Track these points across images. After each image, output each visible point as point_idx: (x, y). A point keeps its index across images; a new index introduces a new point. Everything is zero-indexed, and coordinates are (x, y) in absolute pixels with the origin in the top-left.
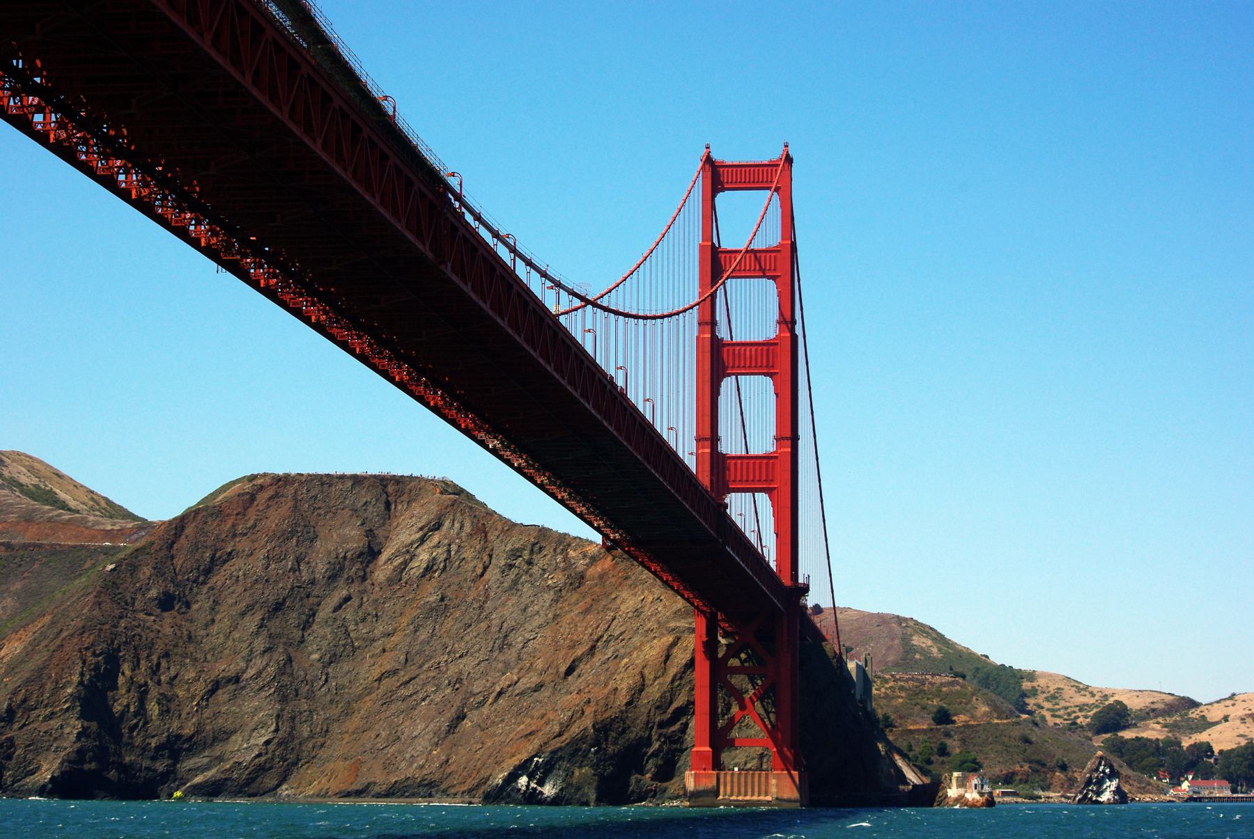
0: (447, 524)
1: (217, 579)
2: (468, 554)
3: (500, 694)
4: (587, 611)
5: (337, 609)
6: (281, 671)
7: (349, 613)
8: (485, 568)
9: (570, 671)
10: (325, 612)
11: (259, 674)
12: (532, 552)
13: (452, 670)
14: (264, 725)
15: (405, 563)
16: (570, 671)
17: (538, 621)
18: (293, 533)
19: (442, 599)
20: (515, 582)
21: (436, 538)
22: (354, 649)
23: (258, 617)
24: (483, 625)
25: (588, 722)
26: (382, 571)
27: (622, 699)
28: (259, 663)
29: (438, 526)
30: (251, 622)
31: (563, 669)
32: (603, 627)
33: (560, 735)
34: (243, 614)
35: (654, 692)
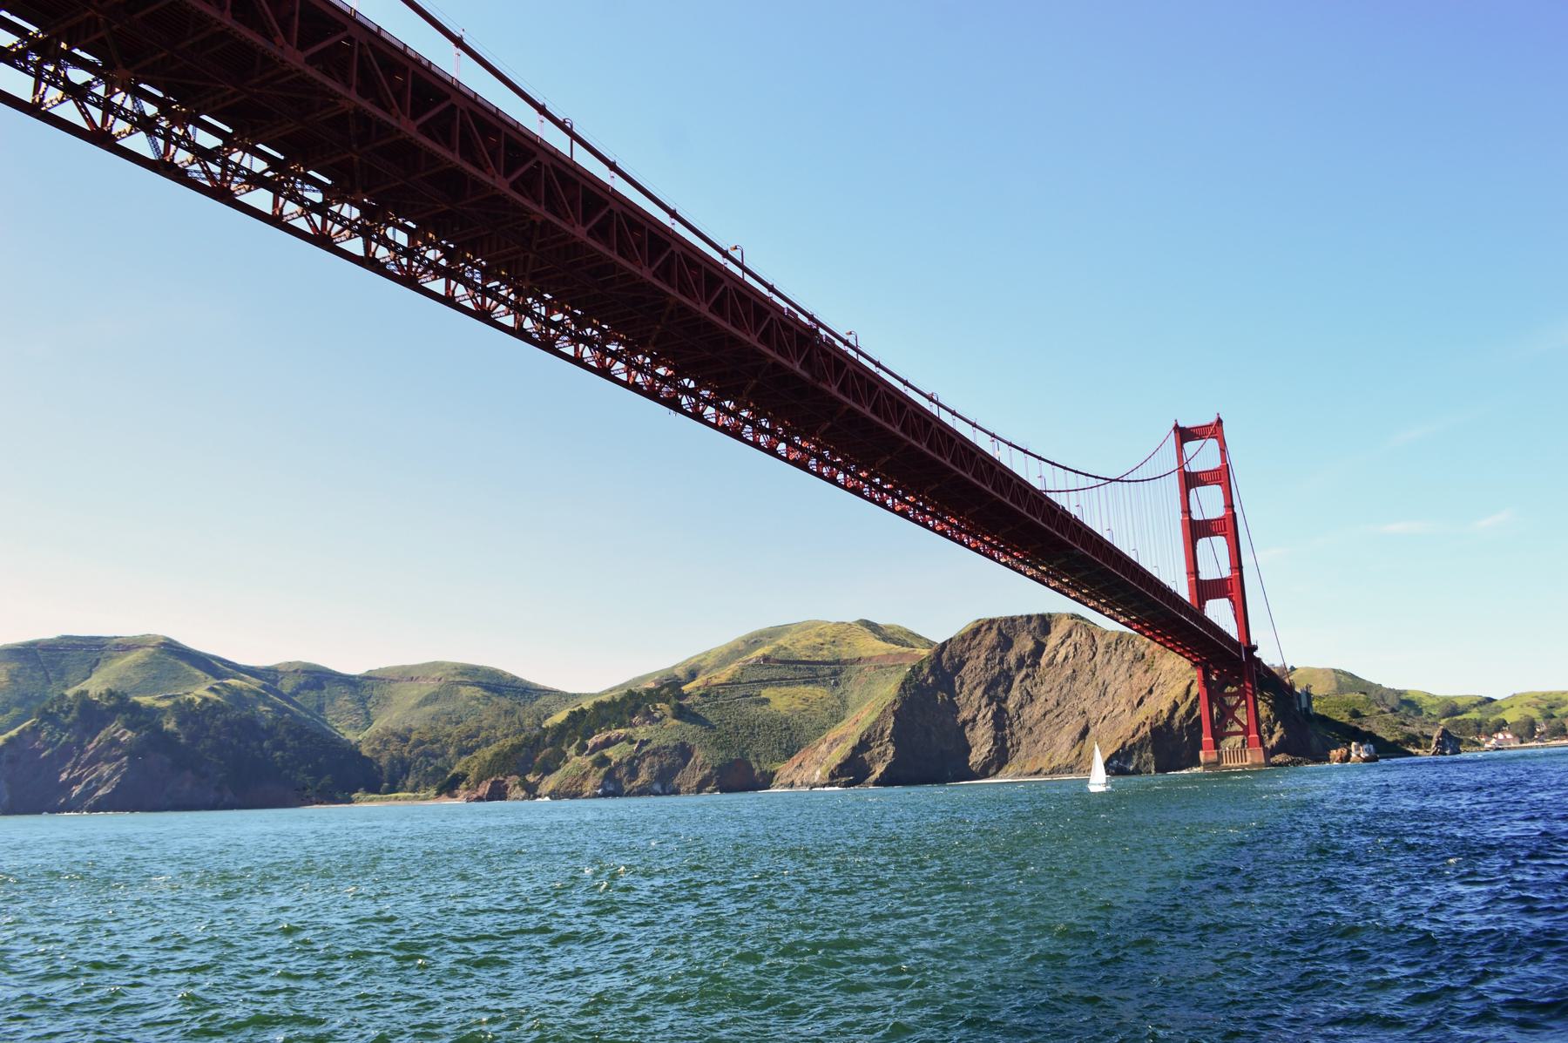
0: (1074, 634)
1: (962, 673)
2: (1086, 648)
3: (1104, 718)
4: (1146, 671)
5: (1022, 681)
6: (994, 716)
7: (1028, 682)
8: (1094, 654)
9: (1141, 702)
10: (1016, 683)
11: (984, 716)
12: (1117, 644)
13: (1081, 707)
14: (986, 742)
15: (1055, 656)
16: (1141, 702)
17: (1121, 678)
18: (999, 645)
19: (1074, 671)
20: (1109, 660)
21: (1069, 641)
22: (1032, 700)
23: (983, 687)
24: (1094, 683)
25: (1147, 728)
26: (1044, 661)
27: (1165, 715)
28: (984, 711)
29: (1069, 635)
30: (979, 692)
31: (1136, 703)
32: (1155, 679)
33: (1133, 736)
34: (975, 688)
35: (1182, 710)
